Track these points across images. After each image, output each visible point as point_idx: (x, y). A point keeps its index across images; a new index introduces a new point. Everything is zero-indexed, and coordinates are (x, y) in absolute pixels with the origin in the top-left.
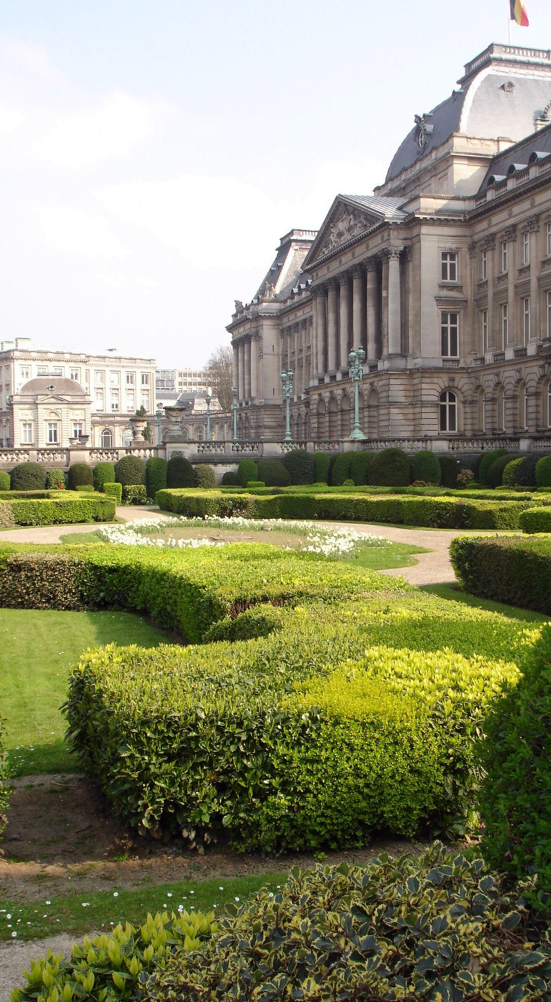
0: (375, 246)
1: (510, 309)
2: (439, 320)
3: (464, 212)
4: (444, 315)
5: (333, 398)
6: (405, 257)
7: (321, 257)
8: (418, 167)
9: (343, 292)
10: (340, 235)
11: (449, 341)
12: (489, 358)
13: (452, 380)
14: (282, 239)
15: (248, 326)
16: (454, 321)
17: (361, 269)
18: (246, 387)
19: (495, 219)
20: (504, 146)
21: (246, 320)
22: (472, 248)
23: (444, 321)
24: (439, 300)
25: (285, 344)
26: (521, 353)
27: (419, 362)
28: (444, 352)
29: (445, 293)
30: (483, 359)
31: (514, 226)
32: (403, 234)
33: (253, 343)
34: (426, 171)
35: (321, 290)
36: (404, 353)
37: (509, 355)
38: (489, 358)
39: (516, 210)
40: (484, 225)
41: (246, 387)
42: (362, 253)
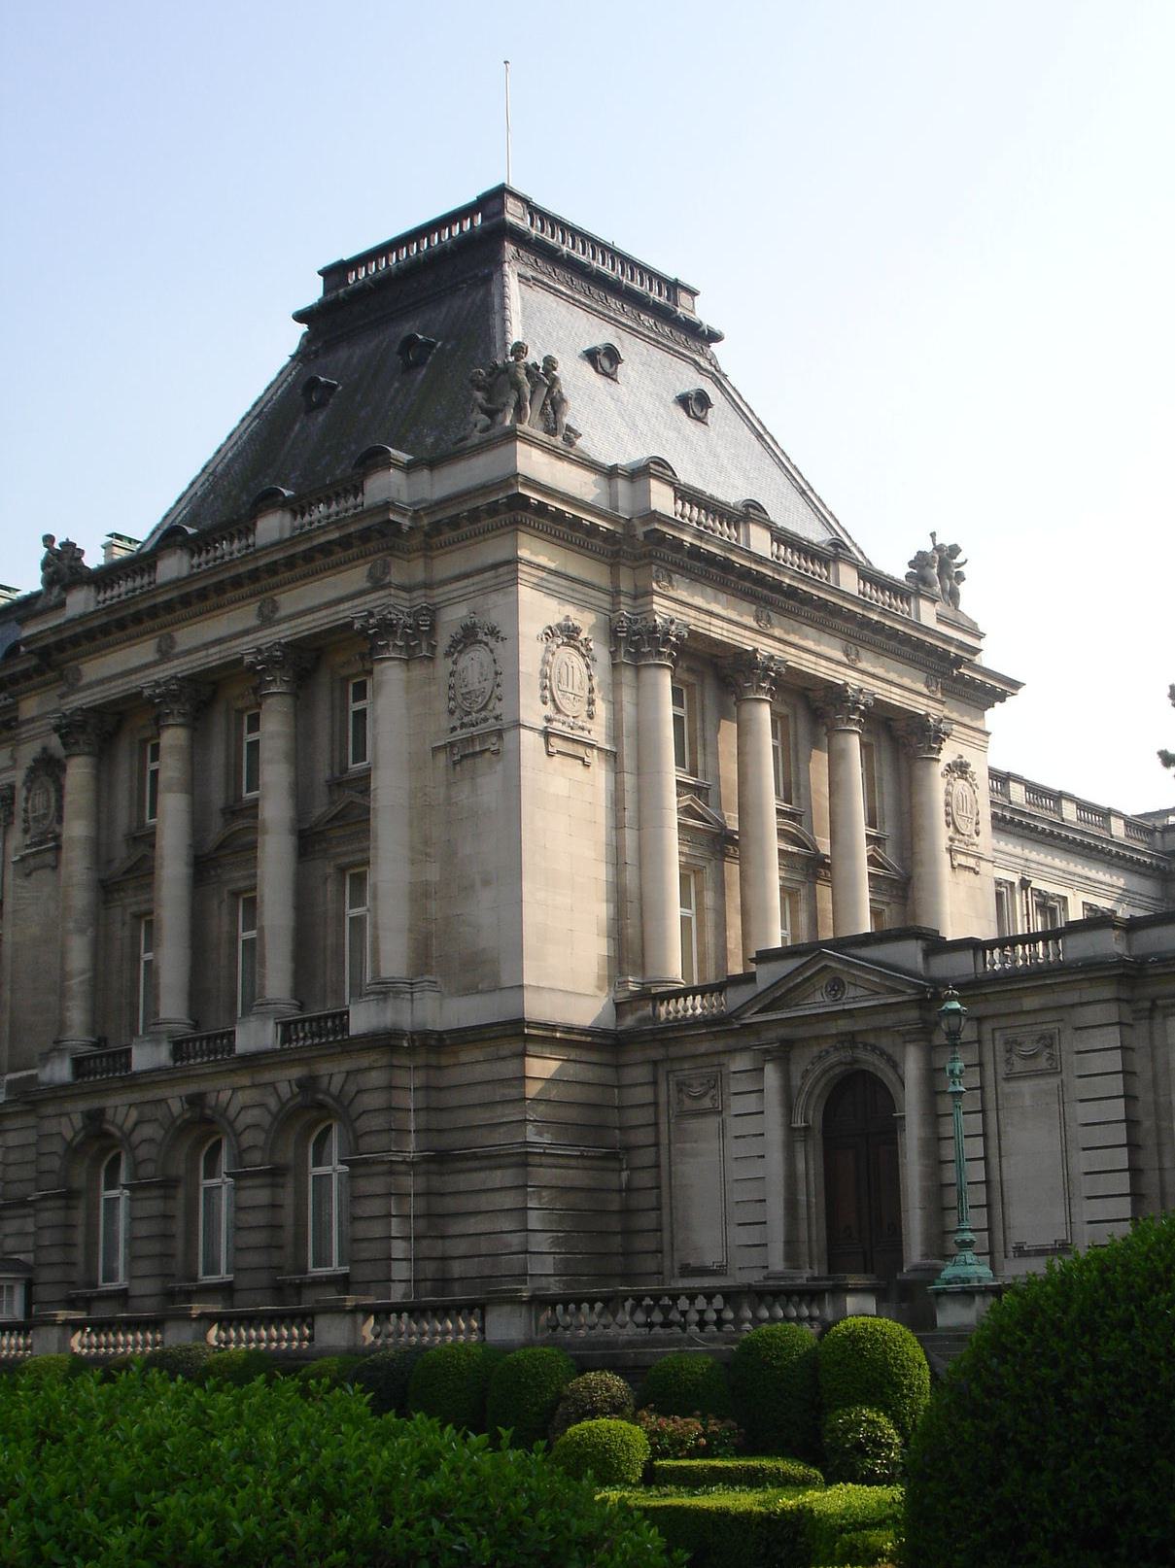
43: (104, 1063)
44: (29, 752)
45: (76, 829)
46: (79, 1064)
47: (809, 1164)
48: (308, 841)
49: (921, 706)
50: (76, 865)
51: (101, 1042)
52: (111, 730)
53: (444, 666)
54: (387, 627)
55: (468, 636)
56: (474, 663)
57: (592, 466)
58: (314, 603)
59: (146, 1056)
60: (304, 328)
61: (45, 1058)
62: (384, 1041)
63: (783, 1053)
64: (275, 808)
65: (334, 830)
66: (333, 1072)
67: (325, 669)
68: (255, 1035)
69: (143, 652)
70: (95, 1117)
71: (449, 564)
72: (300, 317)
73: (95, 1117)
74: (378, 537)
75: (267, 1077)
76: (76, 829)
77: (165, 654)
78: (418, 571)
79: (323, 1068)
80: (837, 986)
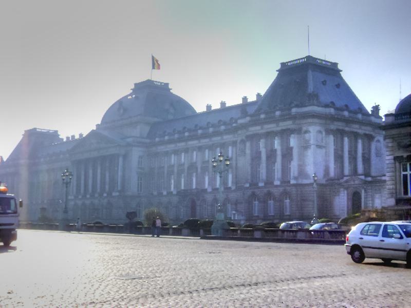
4: (138, 177)
6: (125, 157)
16: (141, 180)
23: (138, 180)
28: (138, 190)
31: (167, 151)
37: (165, 193)
38: (155, 193)
43: (254, 185)
44: (239, 139)
45: (248, 151)
47: (350, 203)
48: (284, 156)
49: (372, 133)
50: (248, 157)
52: (254, 138)
56: (307, 136)
57: (322, 107)
60: (278, 72)
61: (245, 184)
63: (347, 189)
64: (279, 153)
65: (287, 154)
67: (285, 134)
68: (277, 183)
69: (258, 128)
71: (305, 121)
72: (277, 71)
74: (294, 118)
75: (279, 188)
76: (248, 151)
77: (262, 129)
80: (354, 181)
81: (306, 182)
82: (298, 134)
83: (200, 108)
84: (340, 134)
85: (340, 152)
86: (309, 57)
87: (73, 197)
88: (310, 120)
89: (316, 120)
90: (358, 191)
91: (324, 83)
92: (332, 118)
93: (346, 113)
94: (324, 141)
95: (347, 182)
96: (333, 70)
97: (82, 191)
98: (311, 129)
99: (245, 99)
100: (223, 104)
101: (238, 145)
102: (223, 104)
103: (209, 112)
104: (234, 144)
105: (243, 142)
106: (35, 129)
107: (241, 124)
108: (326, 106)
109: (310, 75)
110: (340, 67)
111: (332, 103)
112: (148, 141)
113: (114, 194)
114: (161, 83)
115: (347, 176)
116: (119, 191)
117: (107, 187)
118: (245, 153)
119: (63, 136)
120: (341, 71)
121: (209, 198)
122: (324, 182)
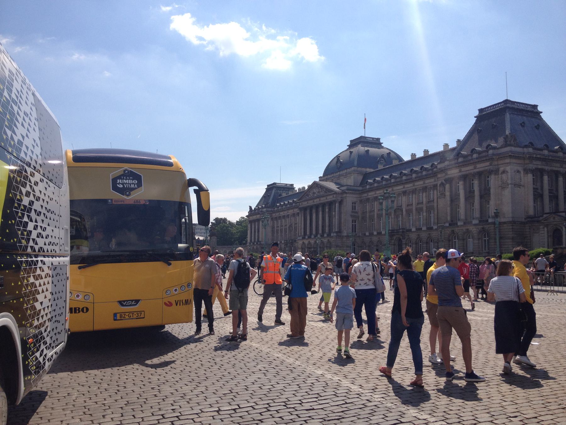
0: (330, 198)
1: (376, 221)
2: (351, 222)
3: (359, 190)
5: (309, 243)
6: (341, 203)
7: (303, 199)
8: (339, 173)
9: (314, 211)
10: (314, 193)
11: (354, 229)
12: (367, 234)
13: (355, 240)
14: (268, 186)
15: (258, 216)
17: (323, 205)
18: (256, 237)
19: (370, 194)
20: (369, 170)
21: (259, 214)
22: (361, 201)
24: (351, 216)
25: (273, 223)
26: (379, 233)
27: (345, 234)
29: (353, 214)
30: (365, 234)
32: (340, 196)
33: (261, 222)
34: (342, 175)
35: (305, 209)
36: (340, 231)
37: (375, 233)
38: (367, 234)
39: (378, 192)
40: (366, 195)
41: (256, 237)
42: (323, 200)
43: (453, 223)
45: (448, 194)
46: (450, 224)
48: (481, 197)
51: (452, 221)
53: (500, 176)
54: (492, 171)
55: (504, 172)
56: (504, 176)
57: (521, 147)
58: (481, 167)
59: (459, 224)
62: (494, 223)
63: (547, 226)
64: (477, 193)
65: (485, 194)
66: (486, 227)
70: (453, 231)
71: (501, 162)
72: (475, 117)
73: (453, 232)
74: (491, 159)
78: (496, 163)
79: (485, 226)
81: (503, 220)
82: (495, 174)
83: (407, 158)
84: (538, 174)
85: (539, 191)
86: (506, 101)
87: (301, 238)
88: (508, 161)
89: (514, 161)
90: (559, 228)
91: (523, 125)
92: (531, 158)
93: (546, 152)
94: (523, 180)
95: (546, 219)
96: (532, 112)
97: (308, 233)
98: (508, 168)
99: (446, 145)
100: (426, 151)
101: (438, 188)
102: (426, 151)
103: (415, 160)
104: (435, 186)
105: (442, 185)
106: (274, 184)
107: (440, 169)
108: (526, 146)
109: (508, 116)
110: (539, 109)
111: (531, 143)
112: (360, 188)
113: (332, 235)
114: (373, 138)
115: (547, 213)
116: (337, 232)
117: (327, 229)
118: (445, 195)
119: (297, 187)
120: (542, 112)
121: (413, 236)
122: (523, 220)
